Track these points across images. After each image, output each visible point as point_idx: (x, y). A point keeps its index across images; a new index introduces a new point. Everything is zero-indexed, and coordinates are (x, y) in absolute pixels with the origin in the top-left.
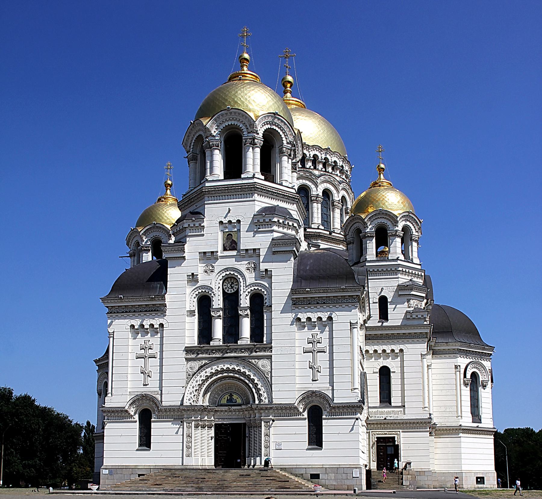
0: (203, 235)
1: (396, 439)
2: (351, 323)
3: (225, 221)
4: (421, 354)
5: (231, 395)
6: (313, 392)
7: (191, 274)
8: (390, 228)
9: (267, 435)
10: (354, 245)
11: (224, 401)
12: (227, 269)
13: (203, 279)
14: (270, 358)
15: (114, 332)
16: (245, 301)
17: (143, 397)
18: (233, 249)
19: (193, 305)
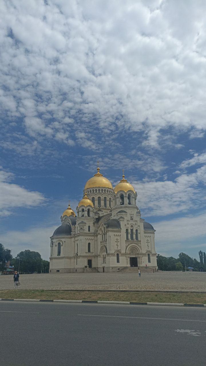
14: (141, 244)
18: (132, 220)
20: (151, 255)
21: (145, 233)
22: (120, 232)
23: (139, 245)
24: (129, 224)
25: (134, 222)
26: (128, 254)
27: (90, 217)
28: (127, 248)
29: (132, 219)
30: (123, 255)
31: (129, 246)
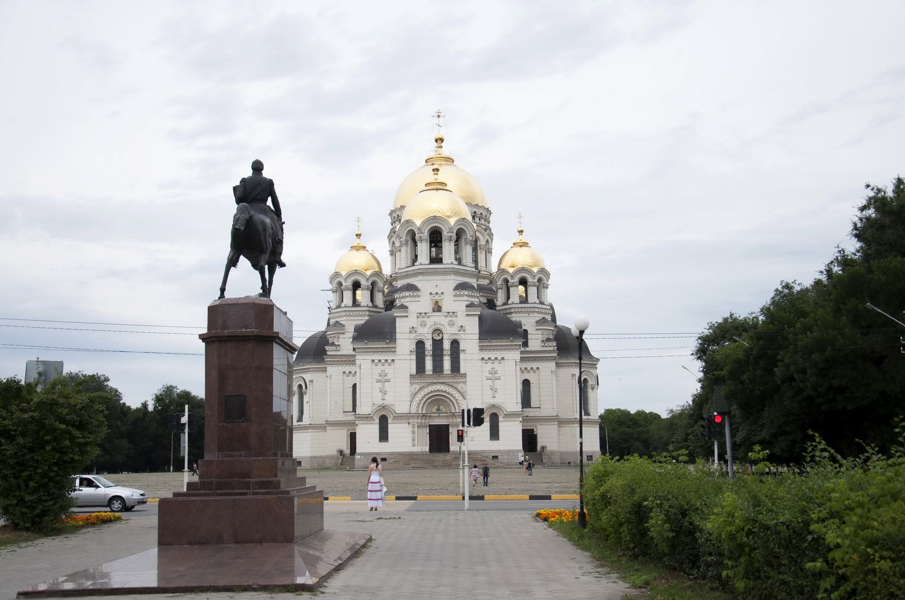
0: (419, 301)
1: (535, 430)
3: (434, 293)
4: (552, 371)
5: (439, 407)
6: (494, 405)
10: (503, 290)
11: (434, 410)
13: (421, 330)
14: (465, 383)
16: (447, 345)
17: (384, 407)
20: (500, 419)
21: (482, 348)
23: (459, 388)
24: (428, 325)
25: (443, 318)
26: (416, 416)
27: (359, 306)
28: (417, 399)
29: (438, 308)
30: (401, 417)
31: (420, 396)
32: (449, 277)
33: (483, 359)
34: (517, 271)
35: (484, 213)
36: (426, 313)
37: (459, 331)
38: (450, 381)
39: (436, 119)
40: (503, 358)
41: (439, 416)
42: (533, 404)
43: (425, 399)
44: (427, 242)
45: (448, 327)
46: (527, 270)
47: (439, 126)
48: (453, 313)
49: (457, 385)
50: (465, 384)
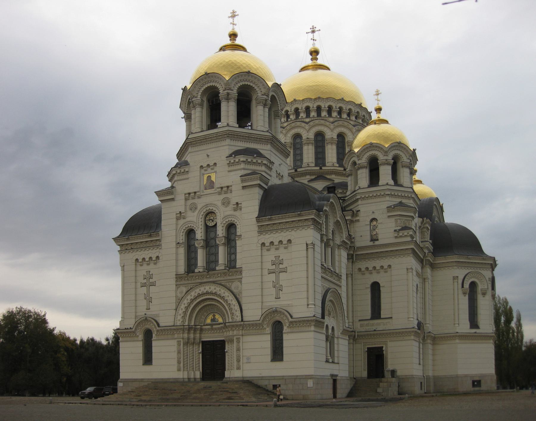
2: (307, 244)
5: (214, 316)
7: (179, 212)
8: (380, 158)
9: (238, 350)
11: (209, 321)
12: (207, 205)
15: (124, 266)
16: (221, 231)
19: (182, 238)
22: (157, 245)
23: (233, 289)
24: (199, 207)
26: (182, 329)
32: (223, 143)
33: (263, 244)
34: (364, 149)
35: (354, 109)
36: (195, 193)
37: (235, 210)
38: (222, 279)
39: (311, 35)
40: (289, 241)
41: (212, 329)
42: (384, 313)
43: (192, 306)
44: (202, 108)
45: (222, 208)
46: (376, 146)
47: (314, 40)
48: (228, 187)
49: (230, 284)
50: (241, 282)
